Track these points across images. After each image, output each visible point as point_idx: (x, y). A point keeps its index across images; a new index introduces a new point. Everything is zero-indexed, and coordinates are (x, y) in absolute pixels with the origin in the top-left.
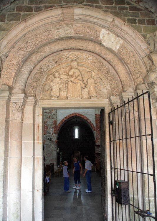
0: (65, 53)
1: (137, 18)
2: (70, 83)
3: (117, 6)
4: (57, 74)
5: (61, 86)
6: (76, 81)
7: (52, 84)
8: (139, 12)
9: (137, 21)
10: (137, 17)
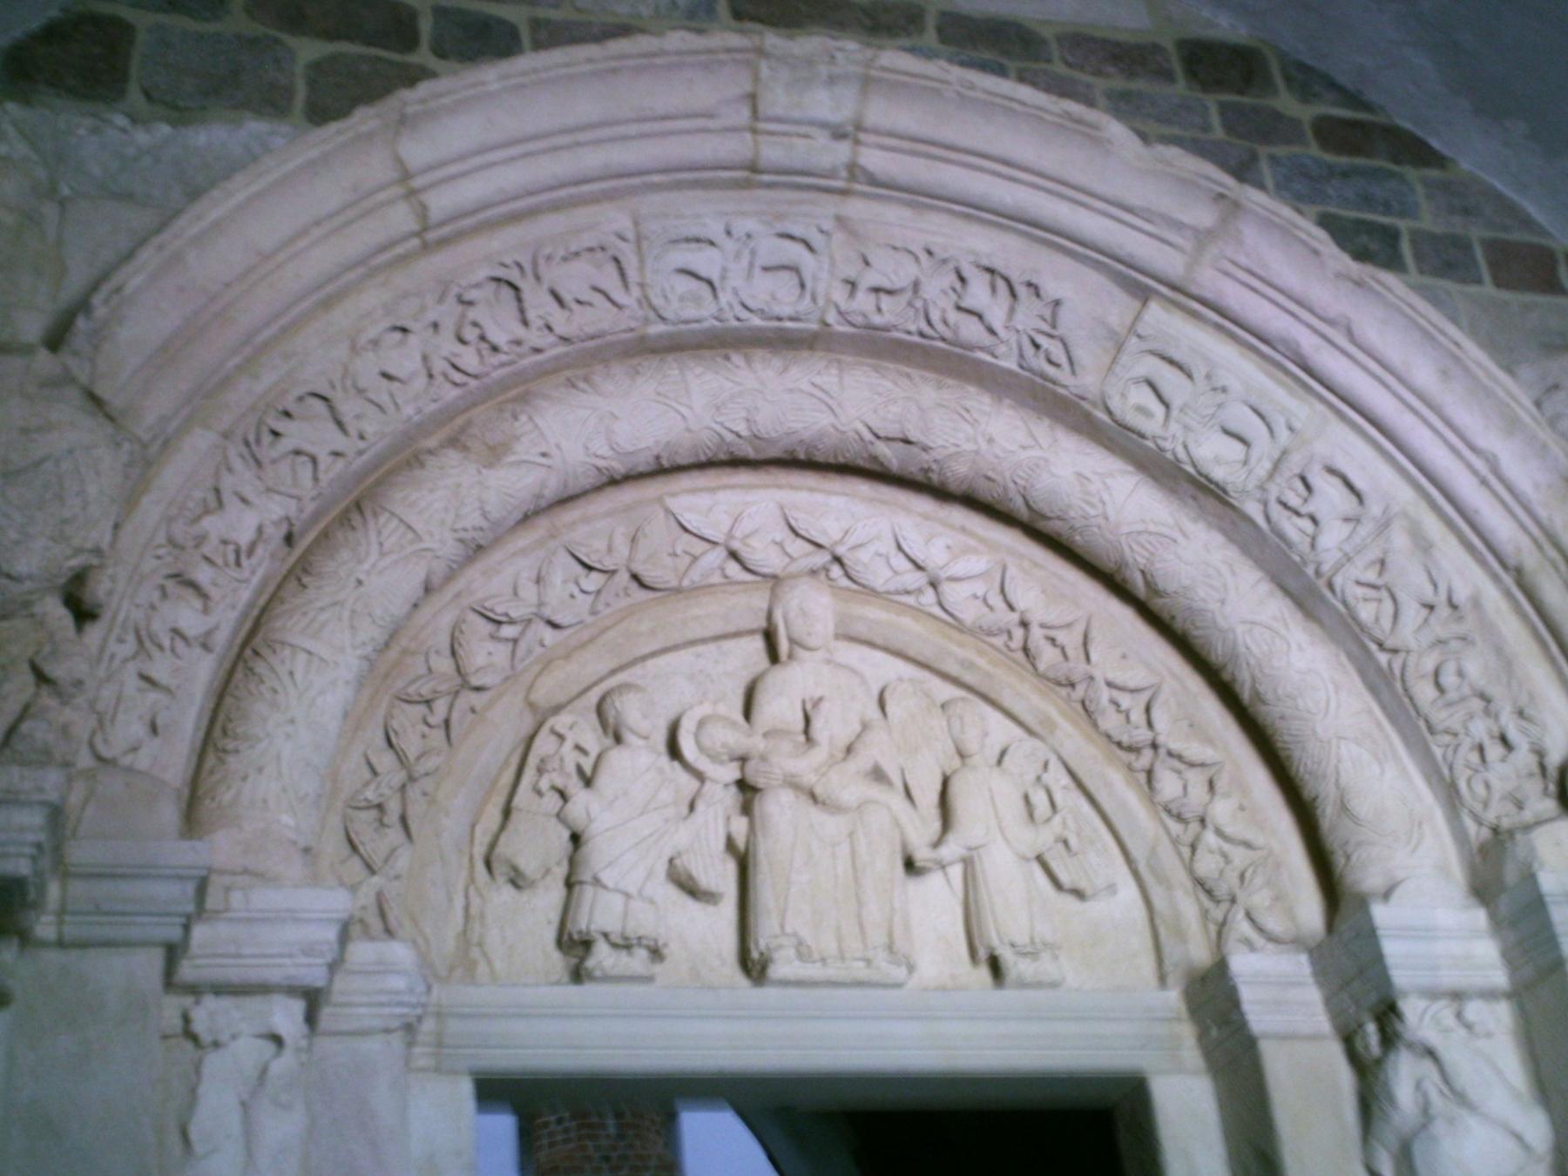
0: (713, 505)
1: (1403, 225)
2: (779, 807)
3: (1212, 102)
4: (630, 710)
5: (681, 837)
6: (848, 786)
7: (582, 803)
8: (1411, 173)
9: (1406, 248)
10: (1403, 214)
